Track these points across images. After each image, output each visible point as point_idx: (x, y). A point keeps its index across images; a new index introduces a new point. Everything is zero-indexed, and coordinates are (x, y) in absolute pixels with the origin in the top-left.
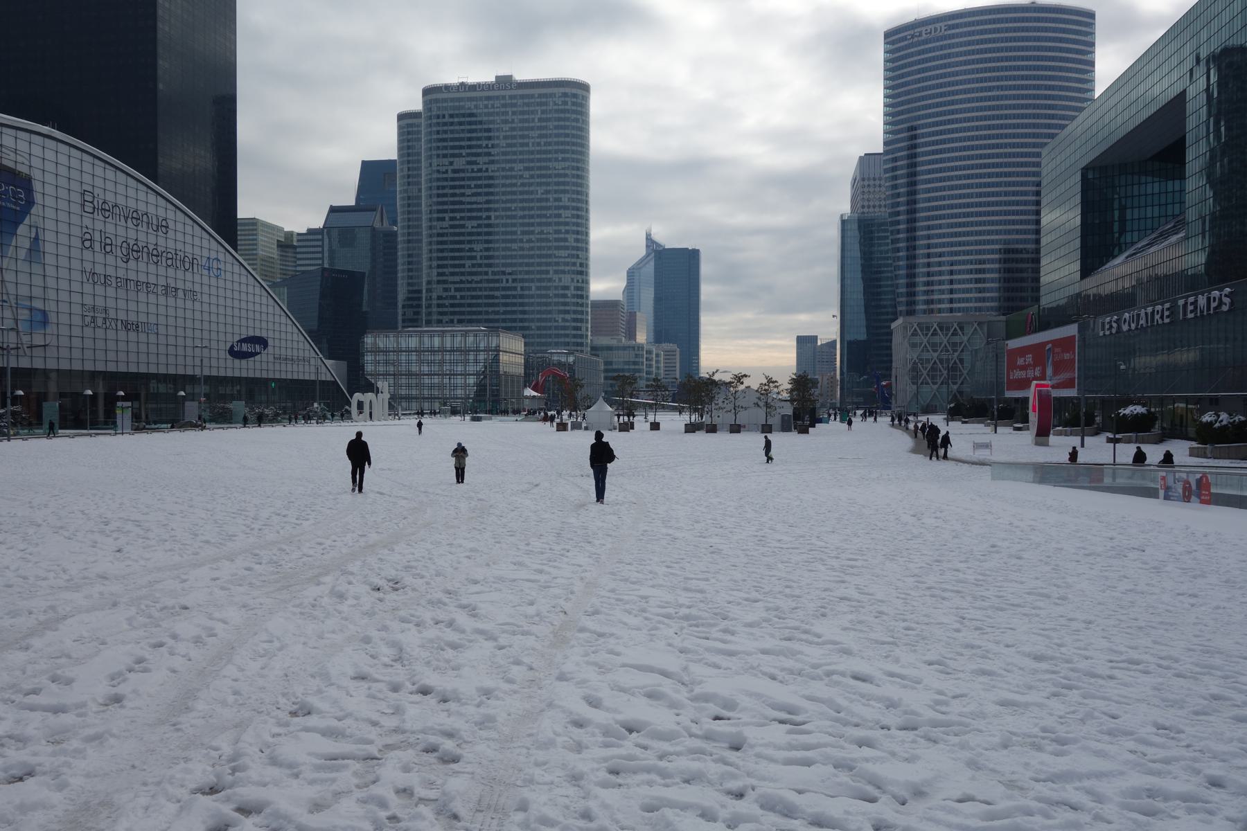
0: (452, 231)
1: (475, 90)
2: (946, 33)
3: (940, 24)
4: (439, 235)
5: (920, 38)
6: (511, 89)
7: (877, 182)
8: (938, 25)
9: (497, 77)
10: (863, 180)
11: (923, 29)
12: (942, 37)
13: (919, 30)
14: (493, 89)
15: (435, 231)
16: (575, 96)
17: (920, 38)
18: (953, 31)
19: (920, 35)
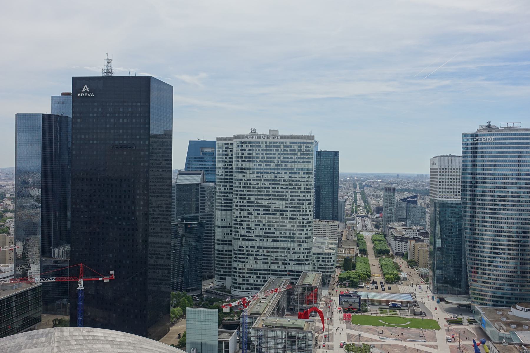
0: (248, 204)
1: (261, 139)
2: (494, 141)
3: (491, 137)
4: (241, 206)
5: (481, 142)
6: (278, 139)
7: (447, 170)
8: (490, 137)
9: (270, 131)
10: (440, 169)
11: (483, 137)
12: (492, 143)
13: (481, 137)
14: (269, 139)
15: (239, 204)
16: (309, 143)
17: (481, 142)
18: (497, 141)
19: (481, 140)
